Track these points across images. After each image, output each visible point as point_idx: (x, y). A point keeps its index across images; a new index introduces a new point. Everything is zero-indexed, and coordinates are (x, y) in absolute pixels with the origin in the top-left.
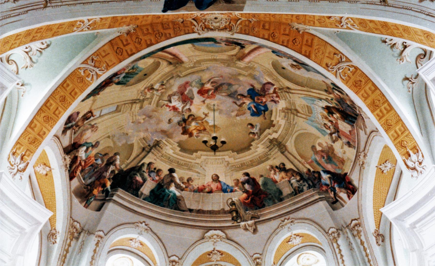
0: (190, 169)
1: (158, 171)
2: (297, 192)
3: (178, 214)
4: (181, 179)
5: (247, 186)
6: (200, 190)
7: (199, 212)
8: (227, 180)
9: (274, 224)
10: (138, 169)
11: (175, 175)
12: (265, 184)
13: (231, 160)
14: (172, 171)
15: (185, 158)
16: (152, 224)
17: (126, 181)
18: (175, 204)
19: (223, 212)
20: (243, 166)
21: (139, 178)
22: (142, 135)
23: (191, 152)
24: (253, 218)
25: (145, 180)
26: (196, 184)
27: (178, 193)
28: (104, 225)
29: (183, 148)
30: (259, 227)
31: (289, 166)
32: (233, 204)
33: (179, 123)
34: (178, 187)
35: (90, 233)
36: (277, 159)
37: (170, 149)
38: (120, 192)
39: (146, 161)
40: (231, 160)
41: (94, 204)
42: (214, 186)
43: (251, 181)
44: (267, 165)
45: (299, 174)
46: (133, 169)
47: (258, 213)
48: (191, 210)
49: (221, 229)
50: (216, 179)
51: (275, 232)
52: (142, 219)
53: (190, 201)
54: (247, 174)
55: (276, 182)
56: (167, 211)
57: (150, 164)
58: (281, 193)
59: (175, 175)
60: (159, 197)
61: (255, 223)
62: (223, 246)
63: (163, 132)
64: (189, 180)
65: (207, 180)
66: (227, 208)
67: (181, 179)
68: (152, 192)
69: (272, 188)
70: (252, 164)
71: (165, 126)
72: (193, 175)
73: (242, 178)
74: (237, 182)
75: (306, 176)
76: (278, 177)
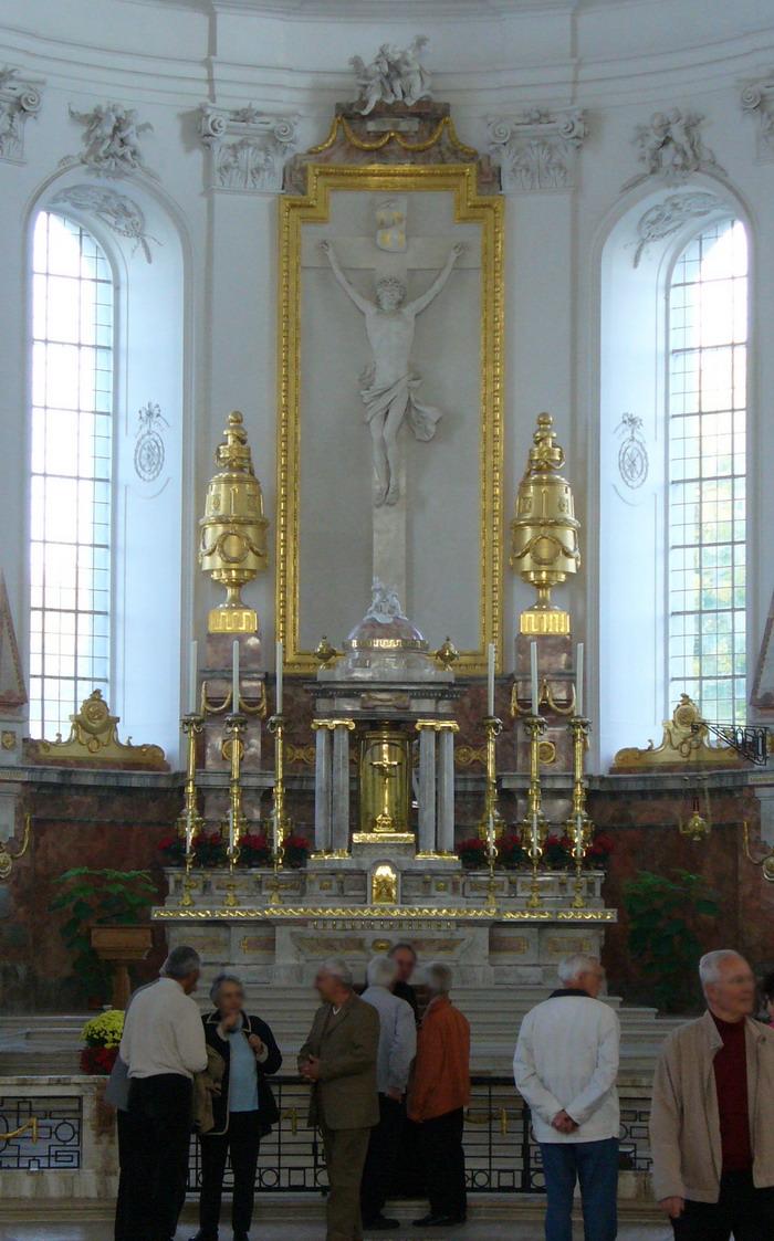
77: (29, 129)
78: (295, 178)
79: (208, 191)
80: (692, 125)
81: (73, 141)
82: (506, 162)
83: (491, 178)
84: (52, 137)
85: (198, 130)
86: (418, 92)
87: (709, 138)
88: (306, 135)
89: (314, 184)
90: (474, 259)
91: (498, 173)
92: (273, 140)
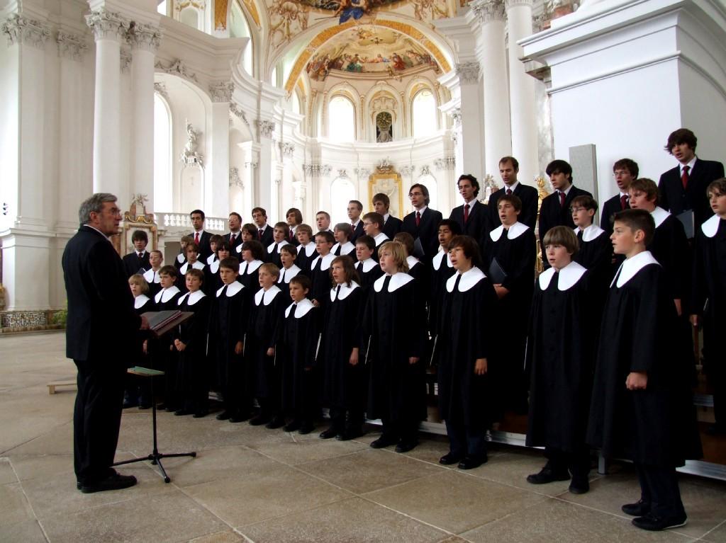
0: (366, 53)
1: (350, 57)
2: (420, 64)
3: (362, 75)
4: (362, 58)
5: (395, 59)
6: (372, 62)
7: (373, 72)
8: (385, 56)
9: (410, 77)
10: (340, 58)
11: (359, 57)
12: (404, 58)
13: (386, 48)
14: (357, 55)
15: (363, 48)
16: (350, 81)
17: (334, 64)
18: (361, 70)
19: (385, 72)
20: (392, 50)
21: (340, 62)
22: (340, 43)
23: (365, 45)
24: (400, 74)
25: (343, 62)
26: (370, 59)
27: (361, 65)
28: (327, 88)
29: (361, 44)
30: (403, 79)
31: (415, 51)
32: (389, 67)
33: (357, 35)
34: (361, 62)
35: (321, 92)
36: (410, 48)
37: (355, 46)
38: (332, 70)
39: (343, 53)
40: (386, 48)
41: (321, 78)
42: (379, 59)
43: (399, 57)
44: (405, 50)
45: (420, 55)
46: (337, 59)
47: (402, 72)
48: (368, 72)
49: (384, 80)
50: (380, 56)
51: (410, 82)
52: (344, 80)
53: (368, 67)
54: (395, 54)
55: (409, 58)
56: (357, 74)
57: (345, 55)
58: (412, 63)
59: (359, 57)
60: (352, 68)
61: (401, 77)
62: (386, 88)
63: (350, 39)
64: (366, 58)
65: (375, 57)
66: (387, 70)
67: (362, 58)
68: (348, 66)
69: (407, 60)
70: (397, 49)
71: (351, 37)
72: (368, 55)
73: (393, 56)
74: (391, 57)
75: (423, 57)
76: (410, 55)
77: (331, 173)
78: (371, 178)
79: (358, 180)
80: (427, 167)
81: (338, 174)
82: (401, 173)
83: (399, 176)
84: (335, 173)
85: (356, 171)
86: (388, 164)
87: (430, 169)
88: (372, 171)
89: (374, 178)
90: (398, 188)
91: (400, 176)
92: (367, 172)
